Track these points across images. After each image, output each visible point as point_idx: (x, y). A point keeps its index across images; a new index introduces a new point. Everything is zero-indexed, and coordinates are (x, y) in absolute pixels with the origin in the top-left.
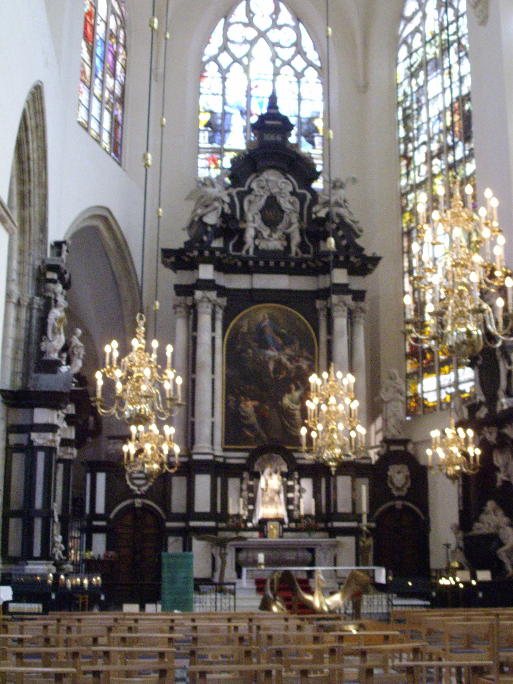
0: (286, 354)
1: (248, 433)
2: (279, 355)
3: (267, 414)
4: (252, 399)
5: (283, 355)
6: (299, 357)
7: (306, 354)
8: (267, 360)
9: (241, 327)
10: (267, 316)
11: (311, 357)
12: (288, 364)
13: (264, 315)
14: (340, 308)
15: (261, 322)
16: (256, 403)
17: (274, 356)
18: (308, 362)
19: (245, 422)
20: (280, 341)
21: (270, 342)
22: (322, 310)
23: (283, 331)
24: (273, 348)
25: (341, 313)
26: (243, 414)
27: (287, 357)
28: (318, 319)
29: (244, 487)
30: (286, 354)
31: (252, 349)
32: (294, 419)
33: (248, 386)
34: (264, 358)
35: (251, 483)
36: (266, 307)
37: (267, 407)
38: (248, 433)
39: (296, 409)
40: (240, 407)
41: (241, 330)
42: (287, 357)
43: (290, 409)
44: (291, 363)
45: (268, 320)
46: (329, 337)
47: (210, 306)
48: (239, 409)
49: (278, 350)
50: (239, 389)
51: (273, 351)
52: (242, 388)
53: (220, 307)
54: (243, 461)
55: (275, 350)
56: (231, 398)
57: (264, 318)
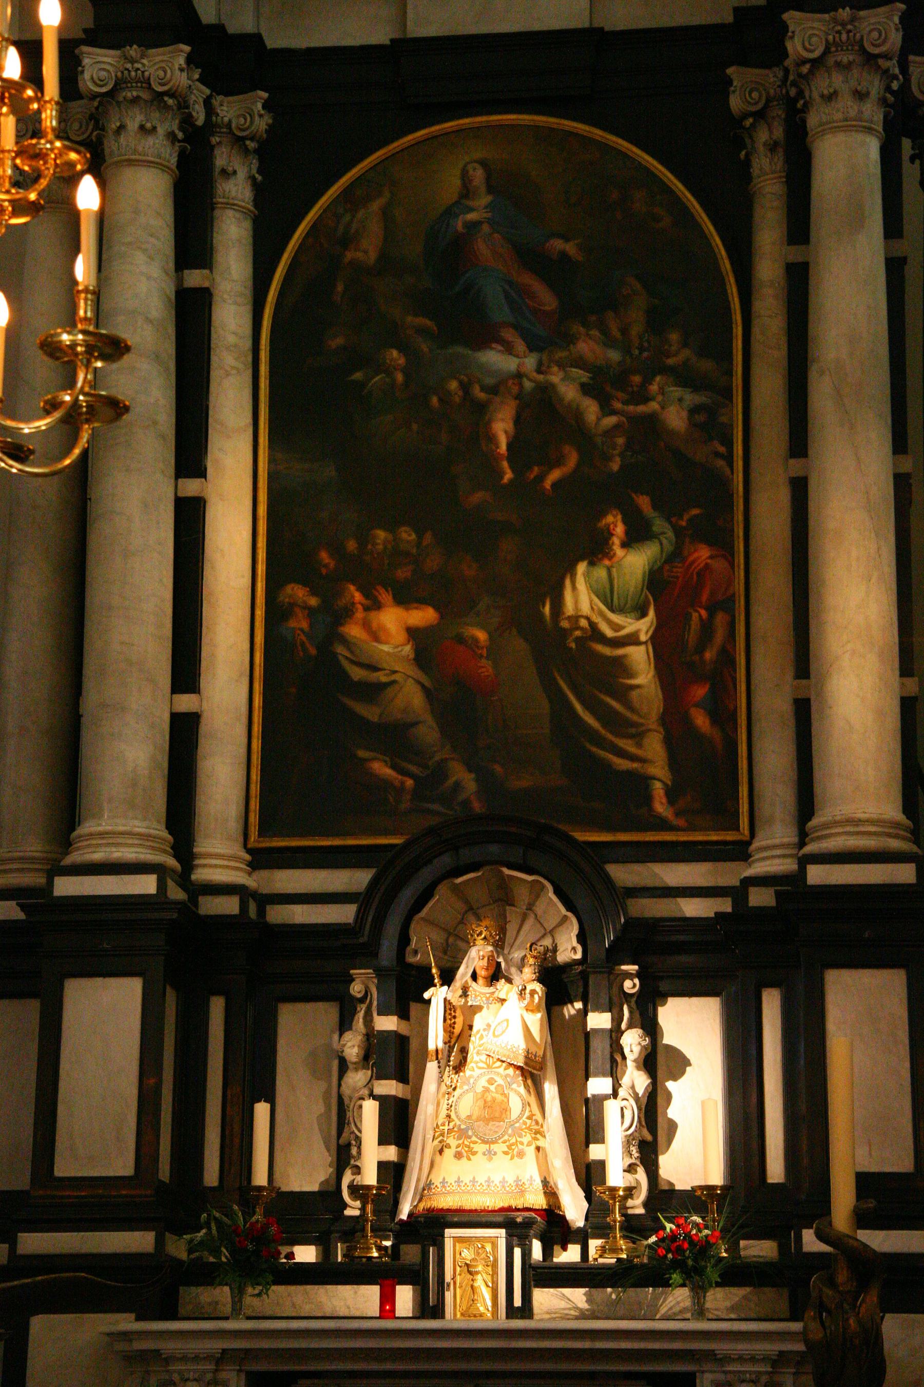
0: (580, 363)
1: (382, 769)
2: (539, 371)
3: (486, 668)
4: (403, 599)
5: (561, 366)
6: (648, 380)
7: (679, 356)
8: (482, 396)
9: (347, 241)
10: (478, 176)
11: (706, 365)
12: (591, 409)
13: (464, 174)
14: (837, 80)
15: (449, 213)
16: (423, 616)
17: (519, 375)
18: (691, 398)
19: (370, 713)
20: (548, 300)
21: (499, 311)
22: (760, 115)
23: (558, 244)
24: (509, 334)
25: (846, 105)
26: (357, 674)
27: (583, 376)
28: (744, 172)
29: (352, 1046)
30: (580, 363)
31: (403, 348)
32: (623, 693)
33: (381, 535)
34: (465, 387)
35: (387, 1023)
36: (476, 131)
37: (481, 636)
38: (382, 769)
39: (632, 640)
40: (344, 641)
41: (349, 255)
42: (583, 376)
43: (595, 634)
44: (606, 409)
45: (485, 200)
46: (795, 254)
47: (168, 124)
48: (340, 650)
49: (532, 347)
50: (337, 550)
51: (509, 349)
52: (352, 545)
53: (238, 141)
54: (344, 914)
55: (520, 346)
56: (297, 592)
57: (467, 192)
